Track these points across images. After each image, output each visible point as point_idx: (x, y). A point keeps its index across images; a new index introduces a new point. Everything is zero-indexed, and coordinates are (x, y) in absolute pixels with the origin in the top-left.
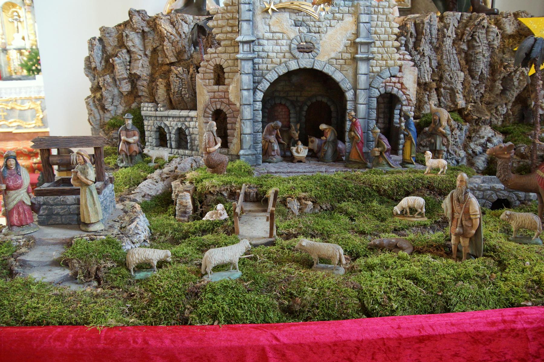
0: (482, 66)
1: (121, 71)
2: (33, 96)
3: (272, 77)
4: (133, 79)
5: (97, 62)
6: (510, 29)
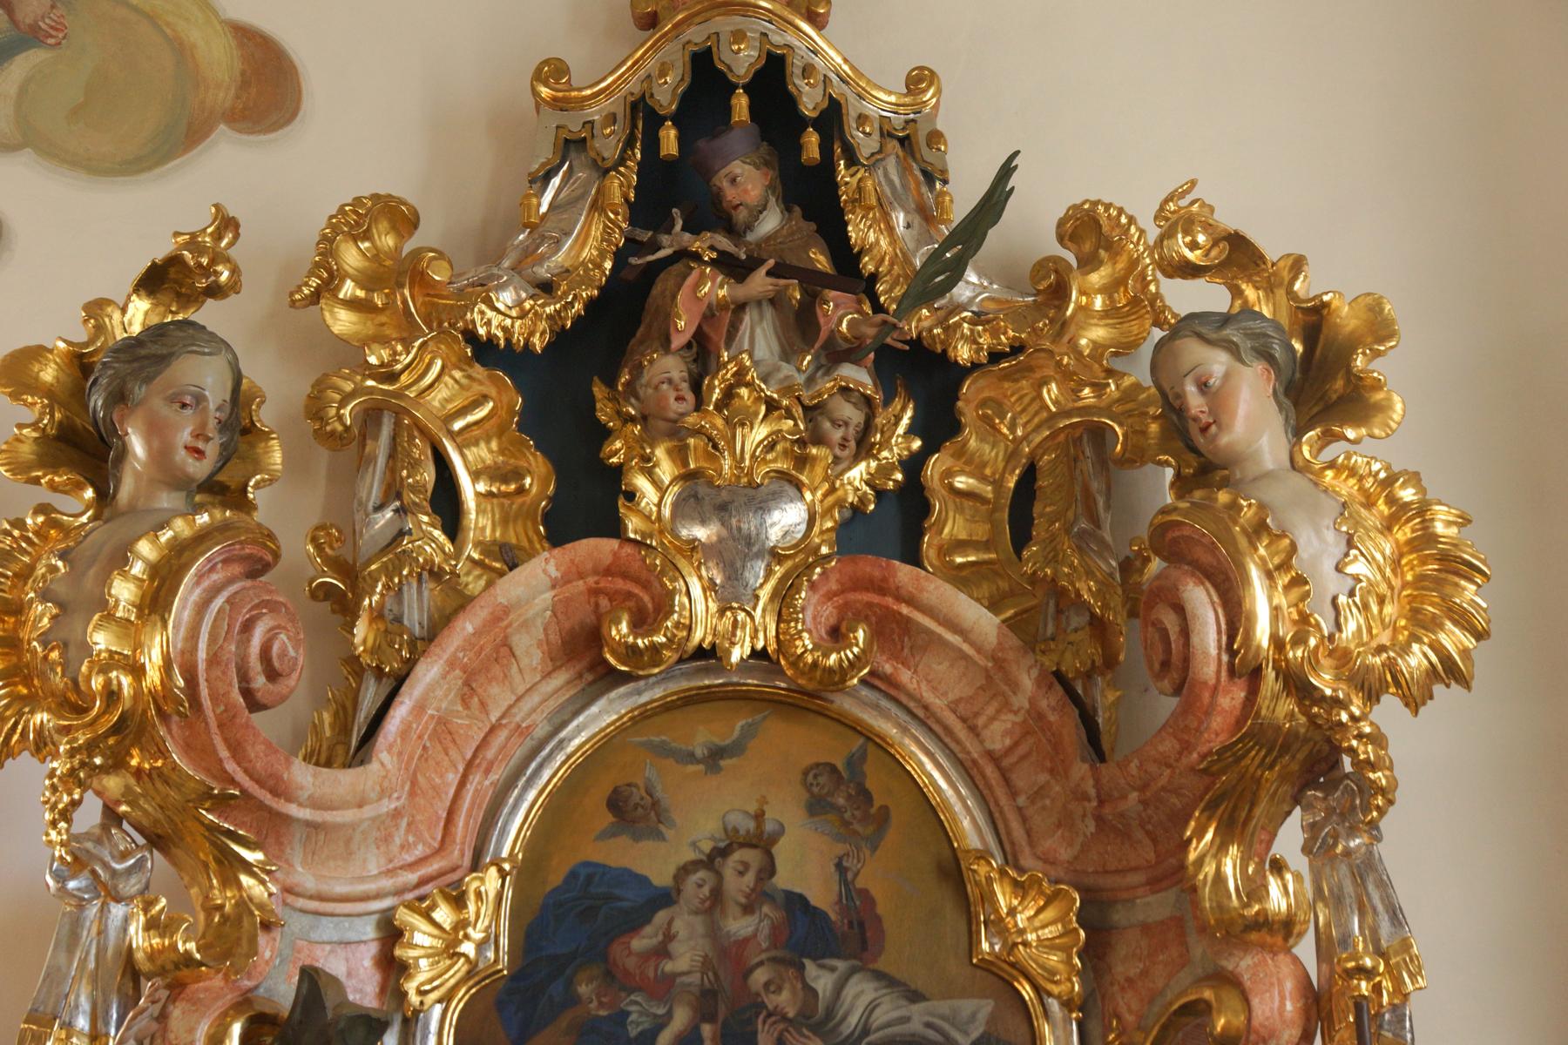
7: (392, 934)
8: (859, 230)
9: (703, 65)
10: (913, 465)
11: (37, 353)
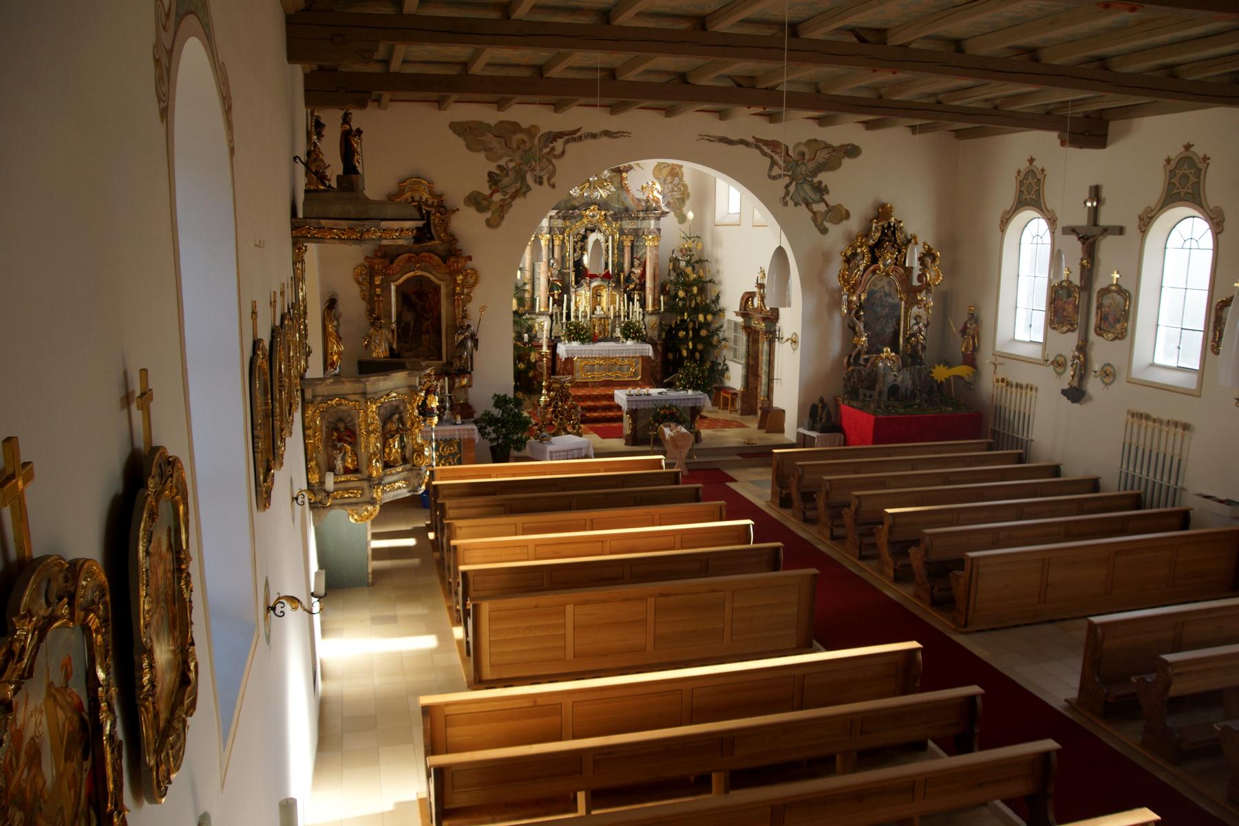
0: (923, 379)
1: (852, 380)
2: (631, 356)
3: (890, 385)
4: (854, 382)
5: (846, 378)
6: (929, 371)
7: (860, 296)
8: (897, 235)
9: (889, 224)
10: (897, 255)
11: (842, 252)
